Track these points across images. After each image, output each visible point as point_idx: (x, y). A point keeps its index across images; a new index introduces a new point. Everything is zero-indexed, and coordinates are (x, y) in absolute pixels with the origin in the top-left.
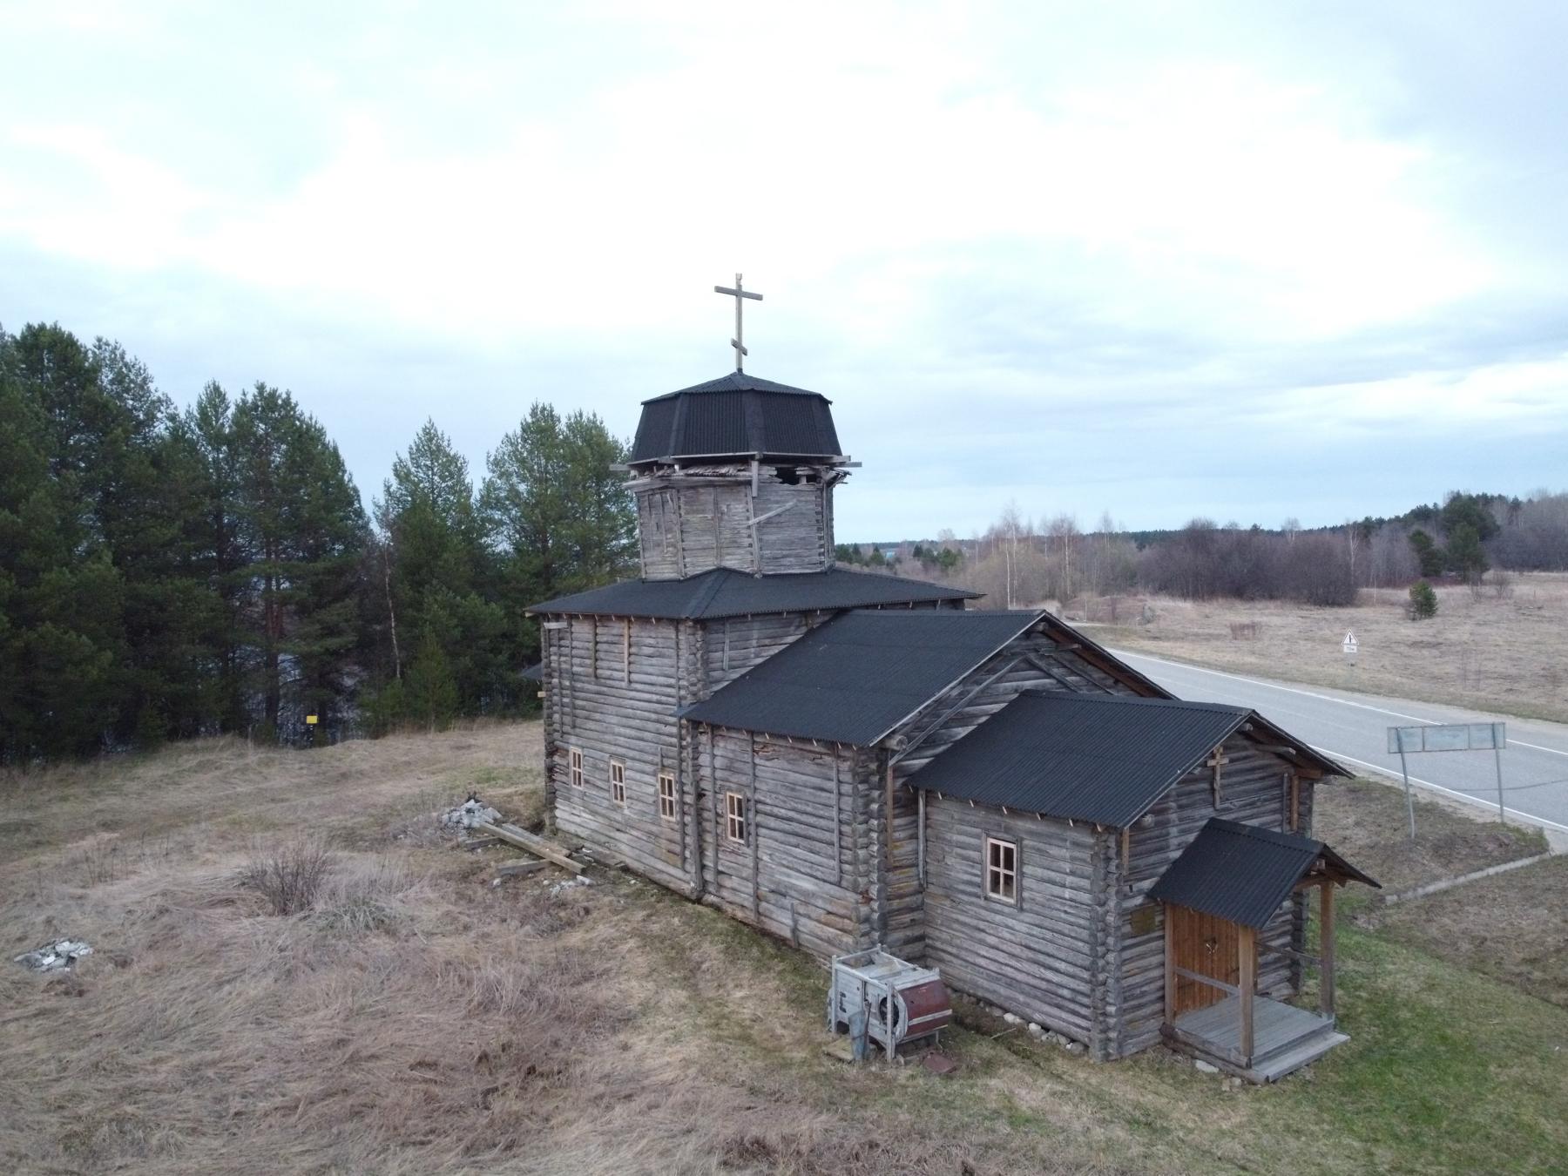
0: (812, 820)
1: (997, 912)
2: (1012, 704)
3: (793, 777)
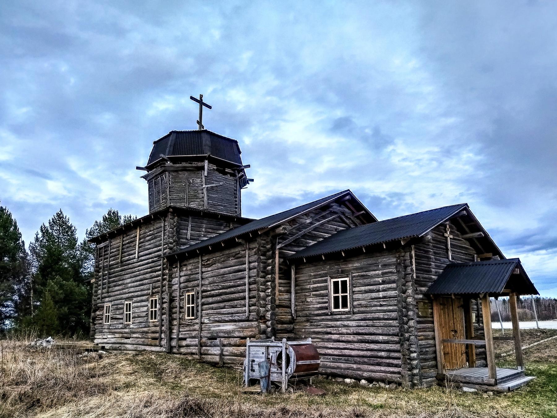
0: (232, 289)
1: (337, 320)
2: (333, 236)
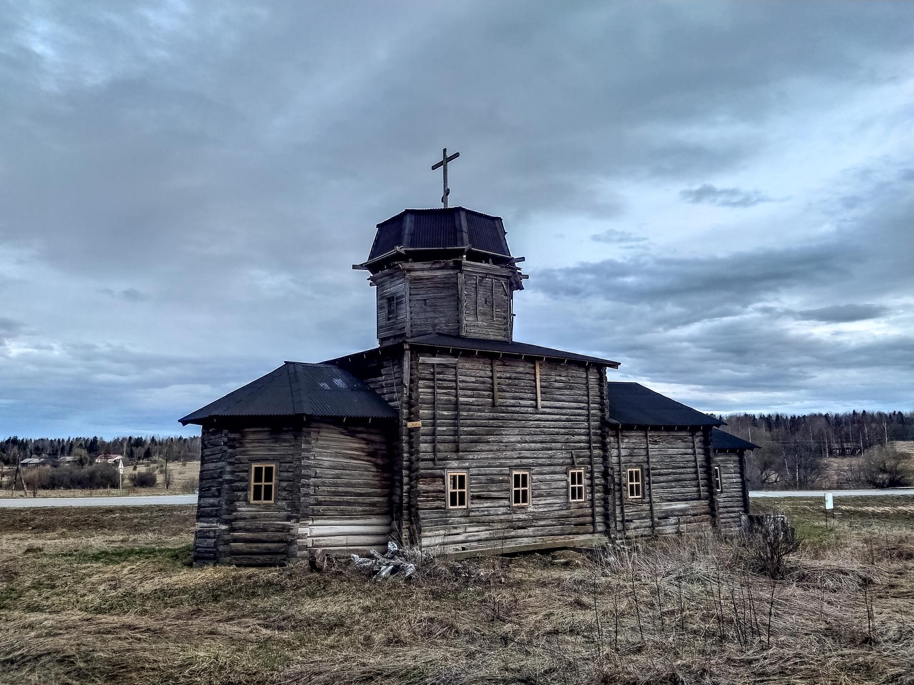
0: (682, 470)
3: (670, 451)
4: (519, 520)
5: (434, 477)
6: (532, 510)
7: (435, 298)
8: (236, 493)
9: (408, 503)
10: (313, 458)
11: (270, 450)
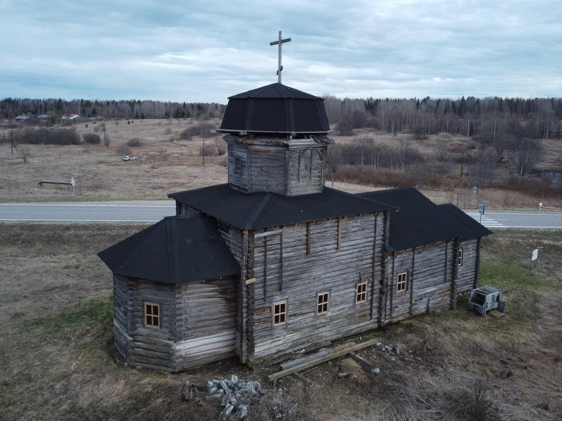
0: (435, 267)
3: (429, 256)
4: (321, 323)
5: (264, 309)
6: (330, 315)
7: (269, 167)
8: (136, 318)
9: (247, 329)
10: (183, 302)
11: (155, 295)
